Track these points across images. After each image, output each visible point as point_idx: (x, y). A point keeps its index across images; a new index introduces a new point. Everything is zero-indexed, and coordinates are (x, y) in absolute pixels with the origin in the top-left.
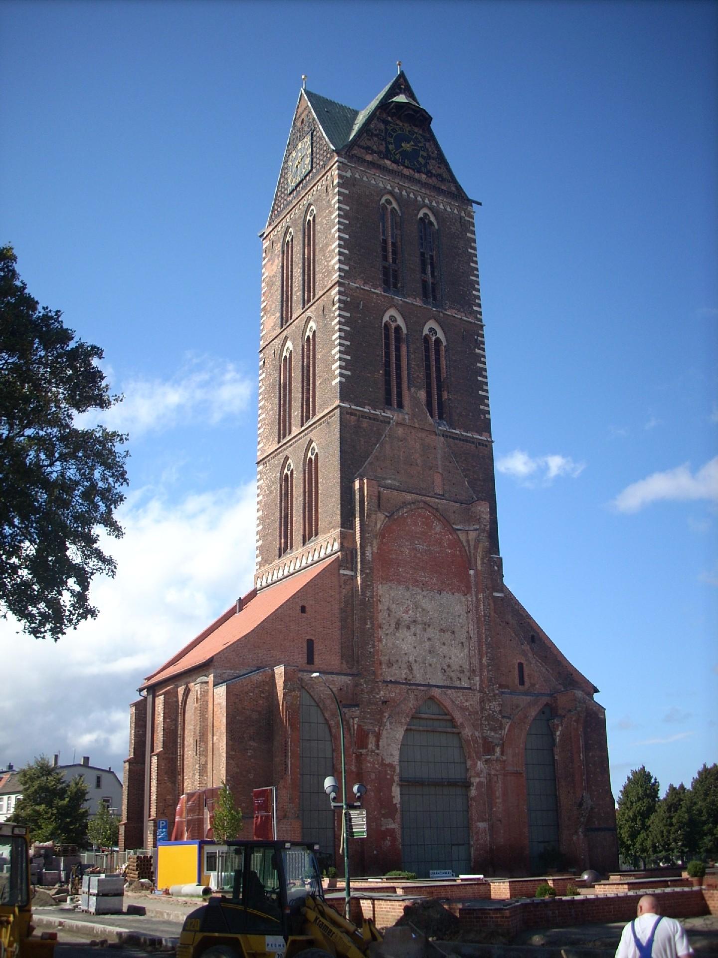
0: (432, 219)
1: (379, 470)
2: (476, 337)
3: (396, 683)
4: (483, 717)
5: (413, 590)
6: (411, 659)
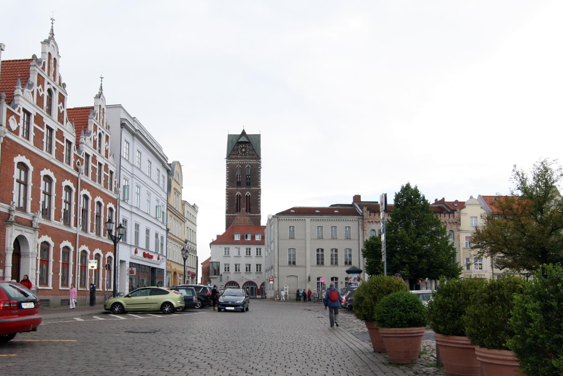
0: (250, 166)
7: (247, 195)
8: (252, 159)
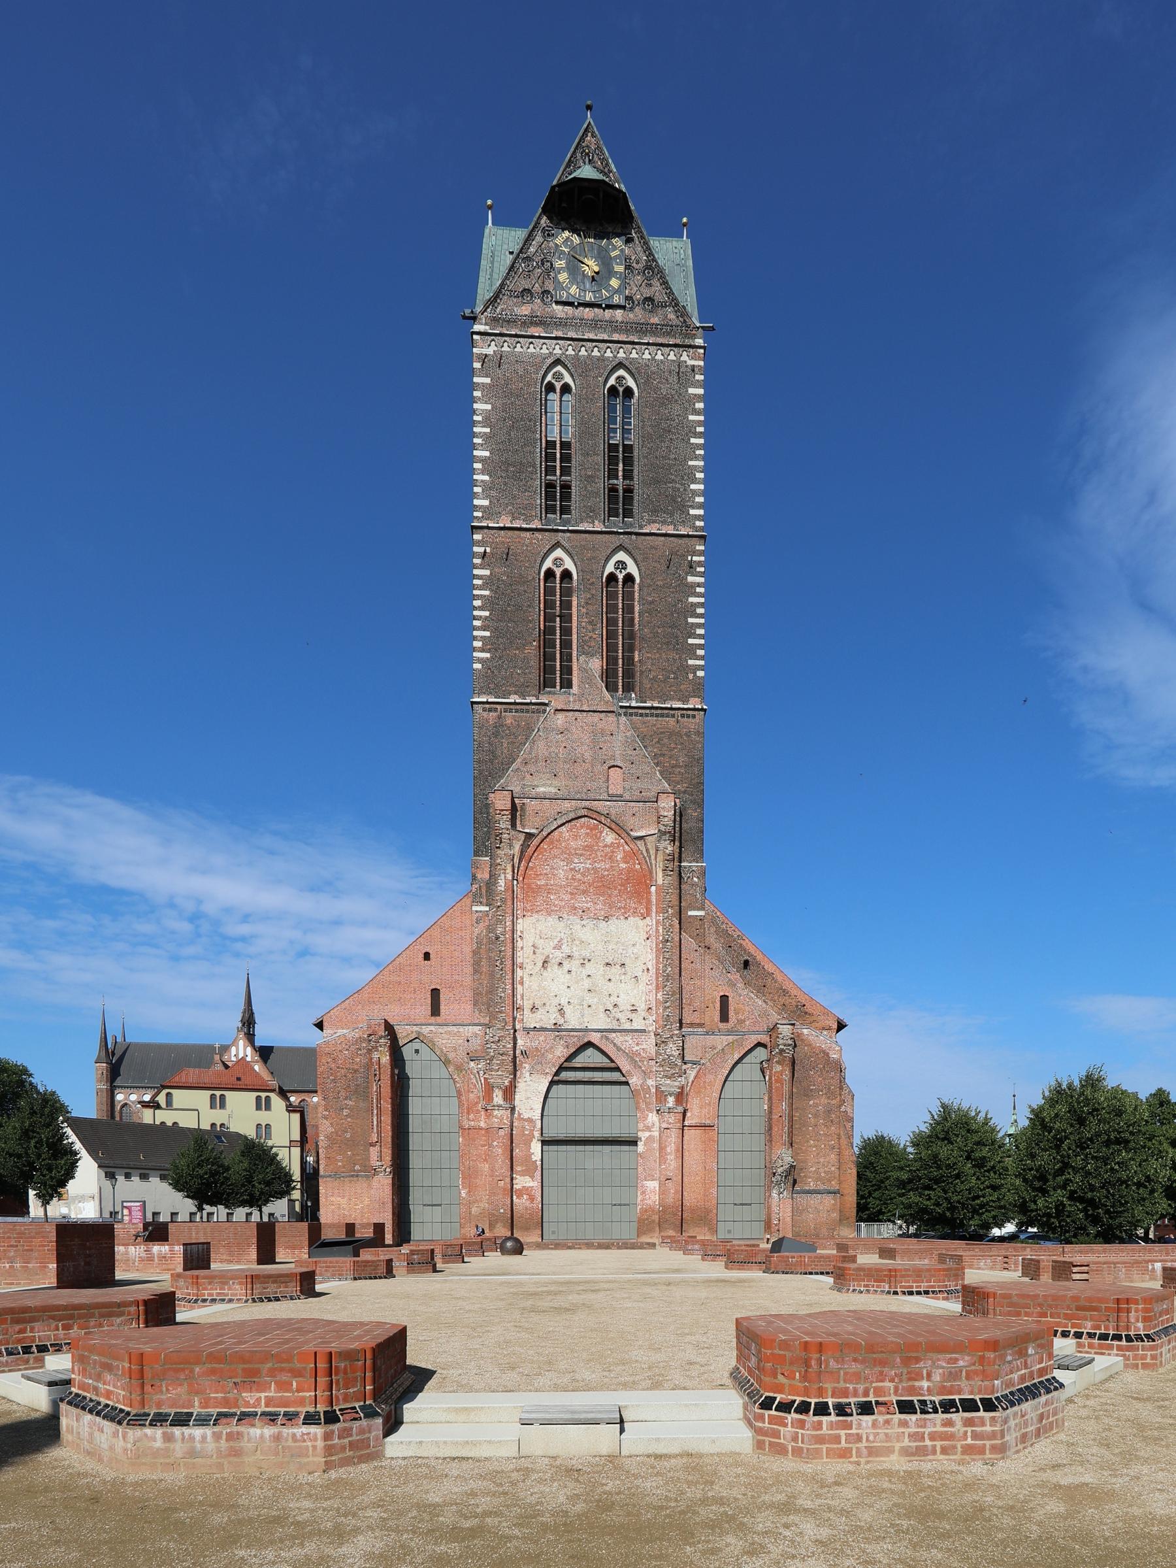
0: (631, 383)
1: (528, 776)
2: (689, 558)
3: (543, 1029)
4: (657, 1062)
5: (568, 919)
6: (564, 1002)
7: (612, 578)
8: (643, 328)
